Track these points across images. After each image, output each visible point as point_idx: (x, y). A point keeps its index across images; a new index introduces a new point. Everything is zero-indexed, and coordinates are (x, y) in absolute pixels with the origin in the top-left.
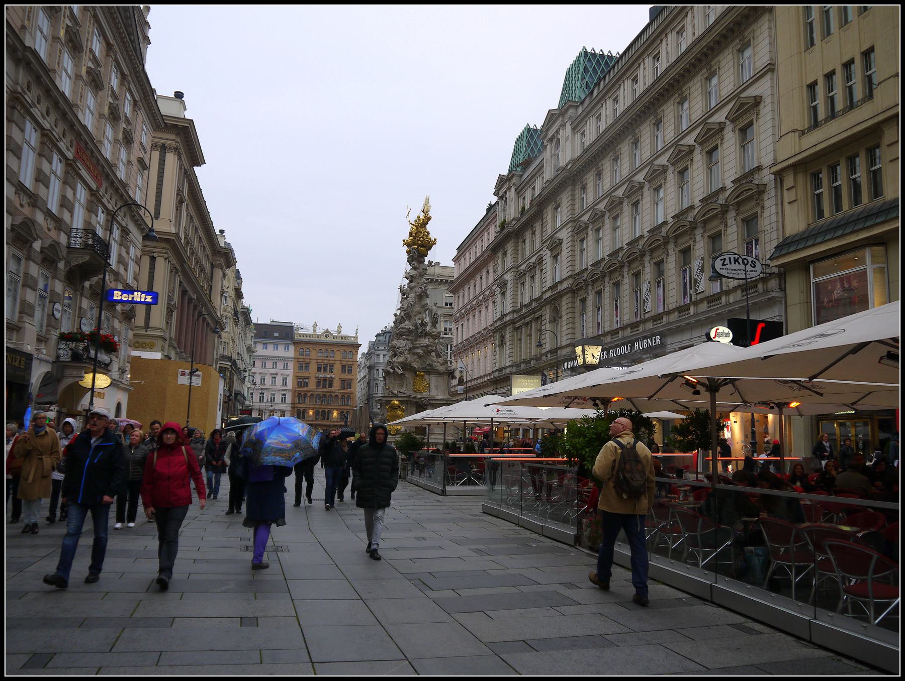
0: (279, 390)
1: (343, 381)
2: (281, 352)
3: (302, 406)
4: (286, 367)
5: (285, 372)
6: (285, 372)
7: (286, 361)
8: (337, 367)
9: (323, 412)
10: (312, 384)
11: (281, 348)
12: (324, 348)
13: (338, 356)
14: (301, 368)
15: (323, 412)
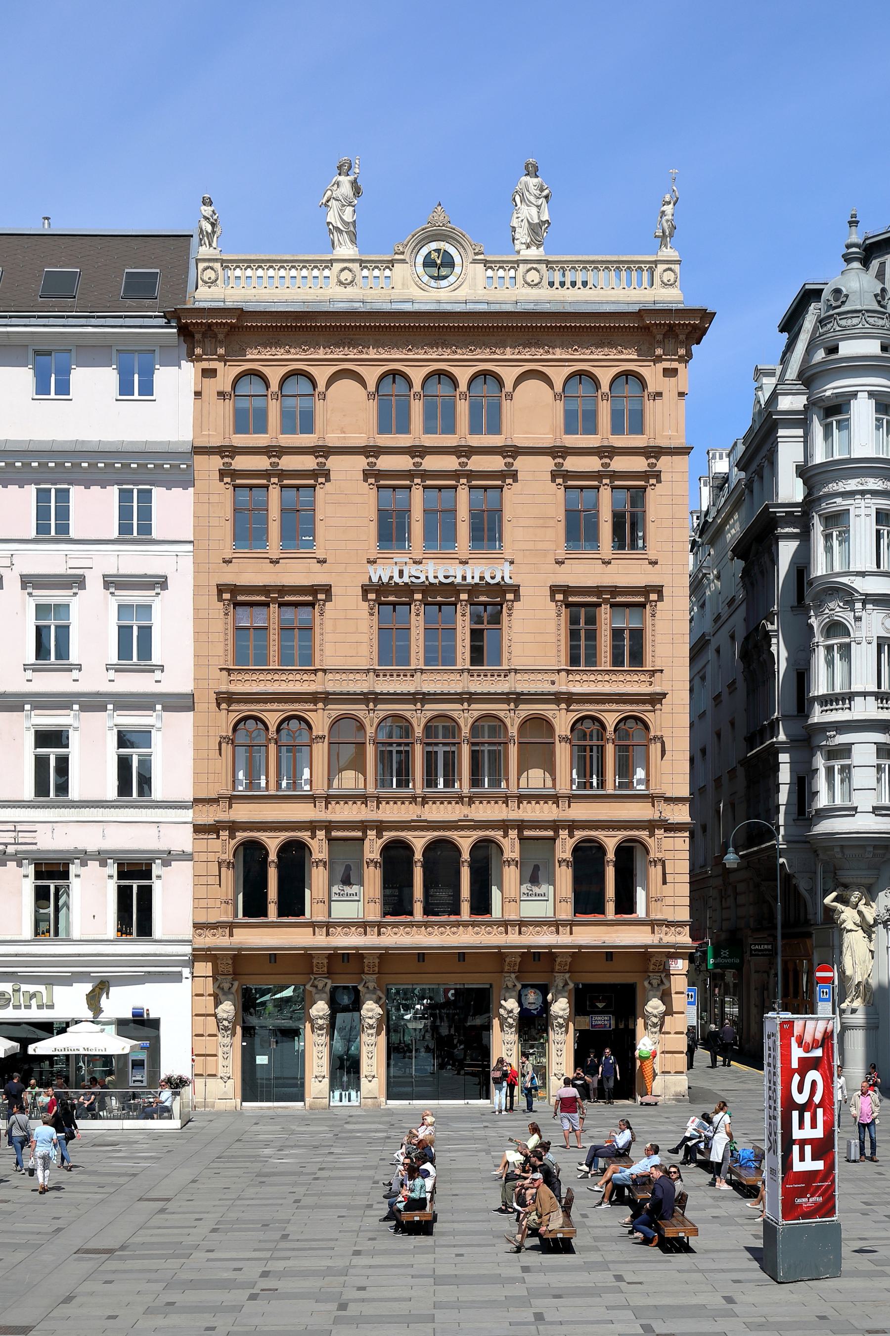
0: (93, 703)
1: (579, 608)
2: (94, 409)
3: (275, 815)
4: (135, 525)
5: (134, 560)
6: (134, 560)
7: (135, 473)
8: (533, 504)
9: (442, 853)
10: (346, 637)
11: (94, 382)
12: (417, 363)
13: (533, 413)
14: (248, 529)
15: (442, 853)
